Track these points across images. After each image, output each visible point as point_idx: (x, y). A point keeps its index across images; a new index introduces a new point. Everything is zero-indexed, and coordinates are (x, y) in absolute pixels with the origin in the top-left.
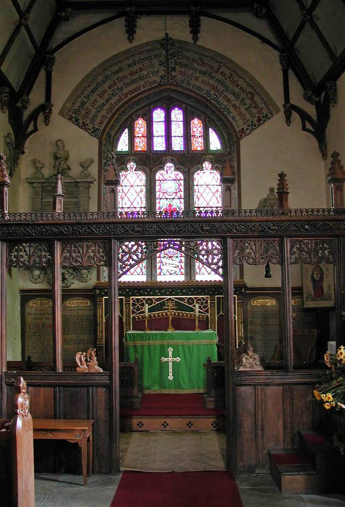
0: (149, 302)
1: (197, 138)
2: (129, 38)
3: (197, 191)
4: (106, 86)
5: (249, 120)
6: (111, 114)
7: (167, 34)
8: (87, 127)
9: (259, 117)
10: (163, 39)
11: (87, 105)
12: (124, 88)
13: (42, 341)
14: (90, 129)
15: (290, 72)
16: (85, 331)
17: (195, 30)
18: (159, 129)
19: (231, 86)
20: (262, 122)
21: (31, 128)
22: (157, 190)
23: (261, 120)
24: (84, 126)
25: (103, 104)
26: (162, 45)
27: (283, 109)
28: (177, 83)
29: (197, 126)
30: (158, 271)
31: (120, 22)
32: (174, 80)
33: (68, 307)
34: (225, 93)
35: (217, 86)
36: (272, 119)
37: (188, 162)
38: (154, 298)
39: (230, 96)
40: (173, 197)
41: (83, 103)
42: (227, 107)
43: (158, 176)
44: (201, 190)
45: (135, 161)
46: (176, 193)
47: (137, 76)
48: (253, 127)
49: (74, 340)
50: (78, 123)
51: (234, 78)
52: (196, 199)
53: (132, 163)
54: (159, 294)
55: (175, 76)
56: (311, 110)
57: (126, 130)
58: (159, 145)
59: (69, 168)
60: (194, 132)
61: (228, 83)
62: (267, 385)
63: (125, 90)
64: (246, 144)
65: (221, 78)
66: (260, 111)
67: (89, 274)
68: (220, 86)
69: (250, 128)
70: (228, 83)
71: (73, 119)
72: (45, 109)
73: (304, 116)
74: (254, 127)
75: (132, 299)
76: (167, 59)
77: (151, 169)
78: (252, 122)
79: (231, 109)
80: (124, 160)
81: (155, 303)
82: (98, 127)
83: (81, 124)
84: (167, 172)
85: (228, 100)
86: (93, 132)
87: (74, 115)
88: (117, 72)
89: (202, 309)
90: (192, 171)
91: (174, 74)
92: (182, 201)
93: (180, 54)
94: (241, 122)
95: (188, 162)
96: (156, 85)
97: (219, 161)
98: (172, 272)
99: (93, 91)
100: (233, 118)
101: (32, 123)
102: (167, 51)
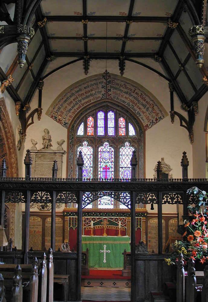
0: (94, 220)
1: (122, 128)
2: (85, 73)
3: (121, 158)
4: (72, 99)
5: (151, 120)
6: (74, 115)
7: (106, 70)
8: (61, 122)
9: (156, 118)
10: (104, 73)
11: (62, 109)
12: (82, 100)
13: (34, 240)
14: (63, 123)
15: (175, 94)
17: (122, 68)
18: (101, 123)
19: (142, 101)
20: (158, 121)
21: (30, 121)
22: (99, 157)
23: (157, 120)
24: (59, 121)
25: (70, 109)
26: (104, 77)
27: (170, 113)
28: (112, 98)
29: (122, 122)
30: (99, 202)
31: (81, 63)
32: (110, 97)
33: (48, 222)
34: (138, 104)
35: (134, 100)
36: (164, 119)
37: (117, 142)
38: (96, 218)
39: (141, 106)
40: (108, 161)
41: (59, 108)
42: (139, 112)
43: (100, 149)
44: (124, 158)
45: (87, 141)
46: (110, 159)
47: (89, 94)
48: (153, 123)
50: (56, 120)
51: (143, 96)
52: (121, 163)
53: (85, 142)
54: (99, 215)
55: (111, 94)
56: (185, 115)
57: (83, 124)
58: (101, 132)
60: (120, 125)
61: (140, 99)
62: (150, 260)
63: (83, 102)
64: (149, 133)
65: (136, 96)
66: (157, 114)
68: (135, 100)
69: (151, 124)
70: (140, 99)
71: (54, 118)
72: (38, 111)
73: (182, 118)
74: (153, 124)
75: (84, 218)
76: (107, 85)
77: (96, 146)
78: (153, 121)
79: (141, 114)
80: (81, 140)
81: (97, 220)
82: (67, 122)
83: (58, 120)
84: (105, 147)
85: (139, 109)
86: (64, 125)
87: (54, 115)
88: (78, 91)
89: (123, 224)
90: (119, 147)
91: (110, 93)
92: (113, 163)
93: (114, 82)
94: (146, 121)
95: (117, 142)
96: (100, 99)
97: (133, 141)
98: (107, 203)
99: (65, 101)
100: (142, 118)
101: (31, 118)
102: (106, 80)
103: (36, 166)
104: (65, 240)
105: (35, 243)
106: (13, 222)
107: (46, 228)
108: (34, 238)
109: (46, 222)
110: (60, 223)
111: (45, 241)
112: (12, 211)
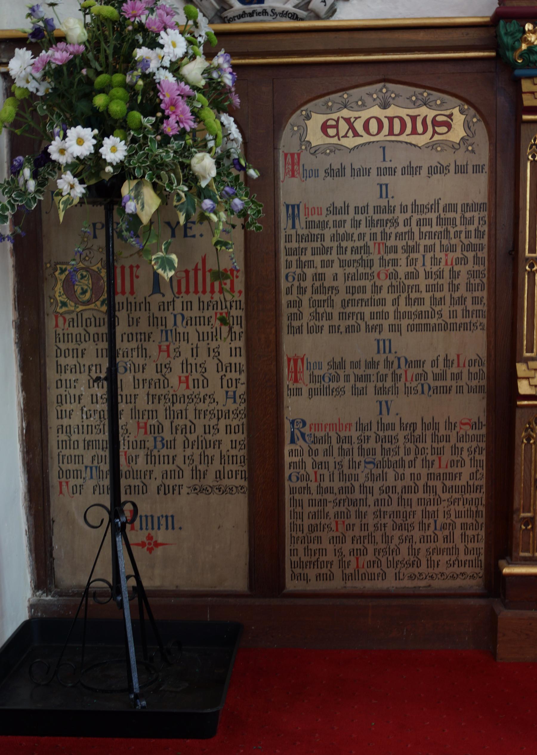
13: (150, 373)
16: (426, 307)
33: (315, 151)
49: (355, 365)
104: (521, 369)
105: (175, 399)
107: (284, 222)
109: (294, 159)
110: (461, 169)
111: (287, 382)
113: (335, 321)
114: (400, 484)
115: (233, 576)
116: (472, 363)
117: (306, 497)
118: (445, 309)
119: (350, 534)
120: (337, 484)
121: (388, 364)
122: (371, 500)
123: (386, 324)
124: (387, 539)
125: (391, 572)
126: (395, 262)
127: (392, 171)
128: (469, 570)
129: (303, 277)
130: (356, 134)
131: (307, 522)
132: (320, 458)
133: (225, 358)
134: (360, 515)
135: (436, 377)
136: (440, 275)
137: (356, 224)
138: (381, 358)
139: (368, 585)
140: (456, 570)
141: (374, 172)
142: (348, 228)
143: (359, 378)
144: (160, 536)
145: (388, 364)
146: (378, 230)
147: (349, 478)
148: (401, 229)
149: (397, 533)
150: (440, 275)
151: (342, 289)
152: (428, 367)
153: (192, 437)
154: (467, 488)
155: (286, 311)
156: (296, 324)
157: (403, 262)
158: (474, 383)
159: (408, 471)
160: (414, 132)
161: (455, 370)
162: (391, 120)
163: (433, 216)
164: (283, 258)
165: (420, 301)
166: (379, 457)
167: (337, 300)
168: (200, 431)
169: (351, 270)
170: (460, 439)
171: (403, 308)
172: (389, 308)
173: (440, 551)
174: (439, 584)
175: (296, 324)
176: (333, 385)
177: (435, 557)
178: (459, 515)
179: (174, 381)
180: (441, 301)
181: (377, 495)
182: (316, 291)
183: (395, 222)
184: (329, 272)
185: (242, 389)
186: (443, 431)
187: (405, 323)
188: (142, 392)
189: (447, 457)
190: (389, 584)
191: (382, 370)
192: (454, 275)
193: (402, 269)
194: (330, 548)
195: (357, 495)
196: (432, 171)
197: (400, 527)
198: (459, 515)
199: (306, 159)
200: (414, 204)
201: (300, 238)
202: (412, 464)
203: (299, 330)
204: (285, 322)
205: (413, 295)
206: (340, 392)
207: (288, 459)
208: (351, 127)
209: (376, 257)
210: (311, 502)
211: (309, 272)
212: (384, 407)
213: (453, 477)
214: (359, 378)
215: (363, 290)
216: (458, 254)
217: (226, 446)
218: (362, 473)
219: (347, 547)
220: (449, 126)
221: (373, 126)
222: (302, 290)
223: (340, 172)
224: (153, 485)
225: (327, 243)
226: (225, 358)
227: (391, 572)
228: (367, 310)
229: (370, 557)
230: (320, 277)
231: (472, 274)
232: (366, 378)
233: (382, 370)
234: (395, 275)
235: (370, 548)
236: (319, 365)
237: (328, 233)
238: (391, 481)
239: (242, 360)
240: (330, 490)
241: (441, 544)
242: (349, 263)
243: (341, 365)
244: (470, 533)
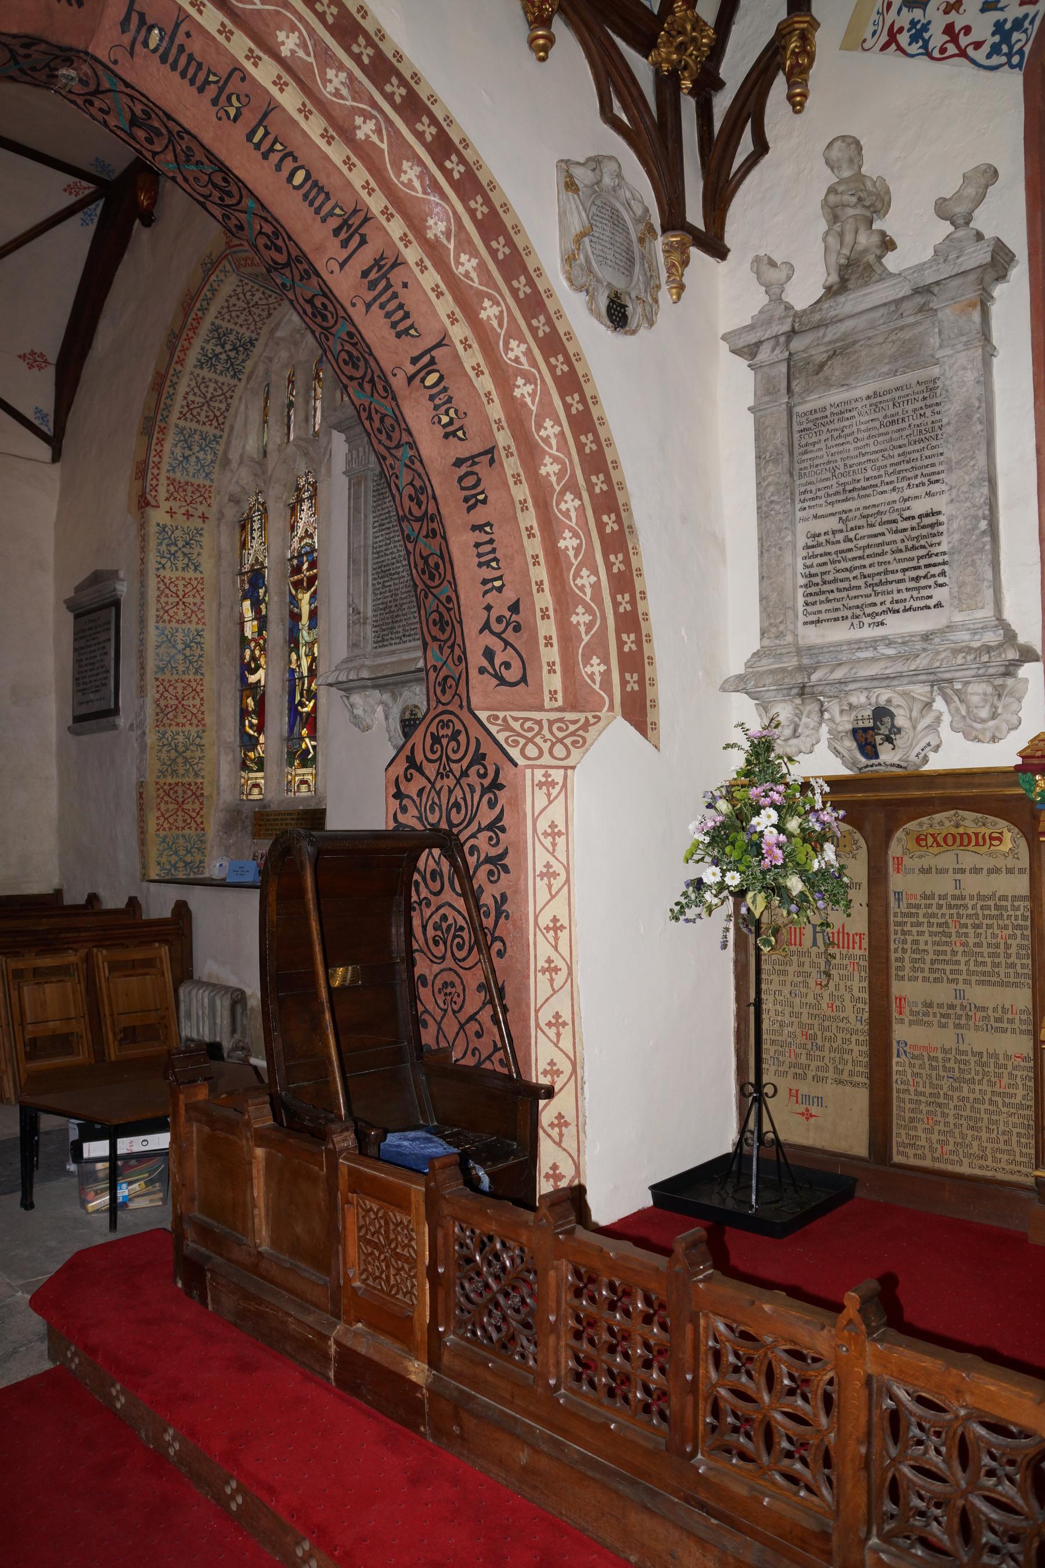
13: (810, 999)
16: (988, 969)
59: (888, 244)
67: (1005, 700)
103: (796, 436)
105: (825, 1018)
106: (557, 867)
107: (893, 903)
108: (812, 982)
109: (899, 861)
110: (1010, 871)
111: (895, 1014)
112: (540, 785)
113: (927, 974)
114: (972, 1096)
115: (861, 1149)
116: (1022, 1012)
117: (907, 1097)
118: (1002, 971)
119: (937, 1128)
120: (928, 1090)
121: (963, 1007)
122: (951, 1106)
123: (961, 978)
124: (963, 1136)
125: (966, 1161)
126: (966, 935)
127: (963, 871)
128: (1024, 1170)
129: (905, 942)
130: (939, 845)
131: (908, 1115)
132: (916, 1070)
133: (856, 994)
134: (944, 1115)
135: (997, 1020)
136: (997, 946)
137: (940, 907)
138: (958, 1002)
139: (950, 1168)
140: (1013, 1167)
141: (951, 871)
142: (934, 909)
143: (943, 1016)
144: (814, 1110)
145: (963, 1007)
146: (954, 911)
147: (936, 1086)
148: (970, 911)
149: (970, 1132)
150: (997, 946)
151: (931, 952)
152: (990, 1012)
153: (835, 1045)
154: (1020, 1106)
155: (894, 964)
156: (901, 973)
157: (971, 935)
158: (1024, 1027)
159: (977, 1087)
160: (977, 844)
161: (1010, 1016)
162: (961, 835)
163: (991, 903)
164: (892, 928)
165: (984, 964)
166: (957, 1075)
167: (928, 958)
168: (840, 1041)
169: (937, 939)
170: (1015, 1068)
171: (972, 968)
172: (963, 967)
173: (1002, 1151)
174: (1000, 1176)
175: (901, 973)
176: (925, 1019)
177: (998, 1155)
178: (1015, 1126)
179: (824, 1006)
180: (998, 965)
181: (956, 1102)
182: (913, 952)
183: (966, 907)
184: (922, 939)
185: (866, 1016)
186: (1002, 1061)
187: (974, 978)
188: (805, 1011)
189: (1005, 1080)
190: (965, 1169)
191: (958, 1011)
192: (1008, 947)
193: (971, 940)
194: (923, 1136)
195: (941, 1100)
196: (991, 871)
197: (972, 1128)
198: (1015, 1126)
199: (906, 861)
200: (978, 894)
201: (903, 915)
202: (980, 1082)
203: (902, 978)
204: (893, 972)
205: (980, 959)
206: (929, 1024)
207: (895, 1068)
208: (935, 840)
209: (953, 931)
210: (911, 1101)
211: (909, 938)
212: (960, 1038)
213: (1013, 1096)
214: (943, 1016)
215: (945, 953)
216: (1010, 931)
217: (856, 1054)
218: (946, 1084)
219: (935, 1137)
220: (1000, 840)
221: (950, 841)
222: (904, 951)
223: (929, 871)
224: (810, 1075)
225: (921, 919)
226: (856, 994)
227: (966, 1161)
228: (948, 968)
229: (951, 1147)
230: (916, 942)
231: (1021, 947)
232: (948, 1016)
233: (958, 1011)
234: (965, 944)
235: (951, 1141)
236: (916, 1004)
237: (921, 912)
238: (965, 1093)
239: (866, 996)
240: (923, 1094)
241: (1002, 1146)
242: (936, 934)
243: (930, 1005)
244: (1023, 1140)
